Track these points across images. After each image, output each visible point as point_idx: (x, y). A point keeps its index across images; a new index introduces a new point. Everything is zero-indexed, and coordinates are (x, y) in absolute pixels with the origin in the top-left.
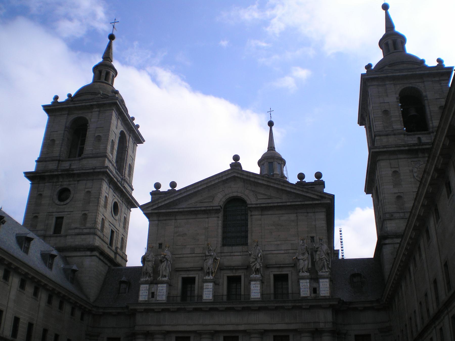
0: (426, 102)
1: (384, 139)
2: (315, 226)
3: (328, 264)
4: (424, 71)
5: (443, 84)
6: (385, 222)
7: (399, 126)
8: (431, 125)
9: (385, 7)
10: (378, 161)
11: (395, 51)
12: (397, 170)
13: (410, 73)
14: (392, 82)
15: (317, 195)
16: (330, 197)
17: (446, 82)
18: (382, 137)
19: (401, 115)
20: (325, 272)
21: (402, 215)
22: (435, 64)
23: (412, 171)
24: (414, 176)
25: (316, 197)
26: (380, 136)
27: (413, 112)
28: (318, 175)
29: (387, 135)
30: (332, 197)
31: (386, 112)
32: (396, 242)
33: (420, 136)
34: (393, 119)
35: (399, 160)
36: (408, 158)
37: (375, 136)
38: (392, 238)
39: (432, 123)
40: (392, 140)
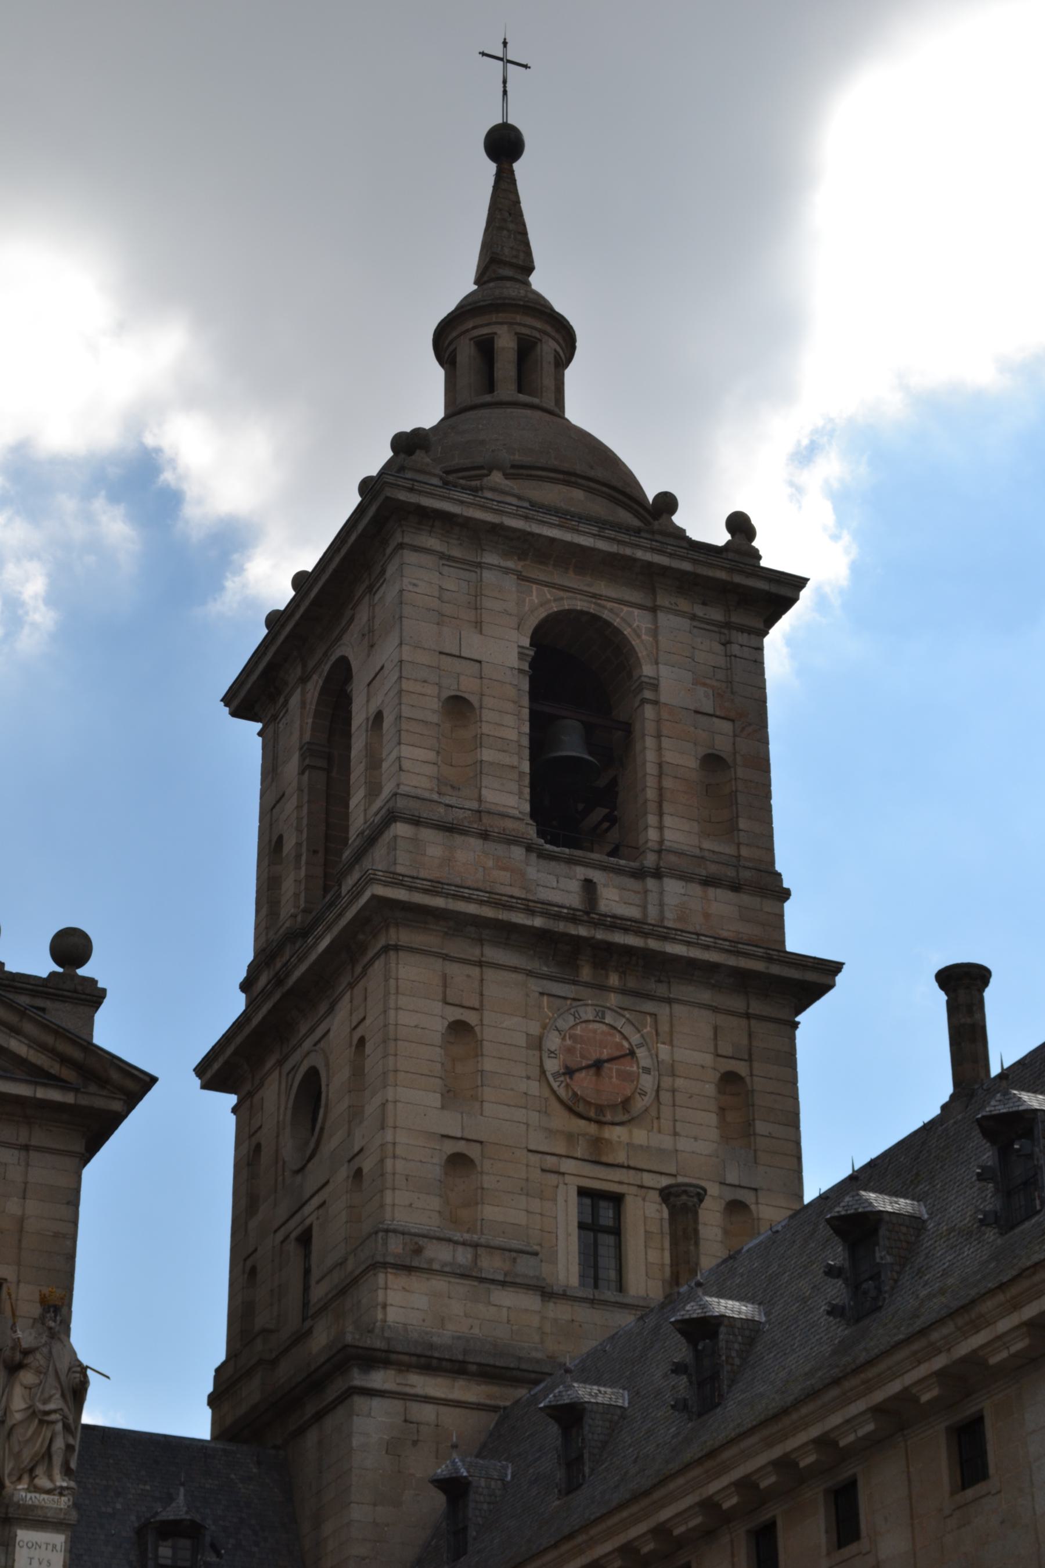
0: (649, 711)
1: (435, 846)
2: (21, 1220)
3: (69, 1448)
4: (671, 555)
5: (735, 649)
6: (381, 1277)
7: (509, 796)
8: (653, 835)
9: (505, 145)
10: (386, 949)
11: (523, 398)
12: (471, 1018)
13: (602, 545)
14: (510, 564)
15: (64, 1060)
16: (131, 1085)
17: (753, 641)
18: (427, 834)
19: (525, 741)
20: (50, 1492)
21: (463, 1257)
22: (720, 537)
23: (537, 1044)
24: (543, 1072)
25: (55, 1068)
26: (416, 822)
27: (571, 745)
28: (71, 947)
29: (450, 829)
30: (136, 1084)
31: (458, 707)
32: (419, 1391)
33: (597, 876)
34: (487, 755)
35: (490, 974)
36: (530, 973)
37: (391, 817)
38: (404, 1368)
39: (661, 828)
40: (469, 861)
